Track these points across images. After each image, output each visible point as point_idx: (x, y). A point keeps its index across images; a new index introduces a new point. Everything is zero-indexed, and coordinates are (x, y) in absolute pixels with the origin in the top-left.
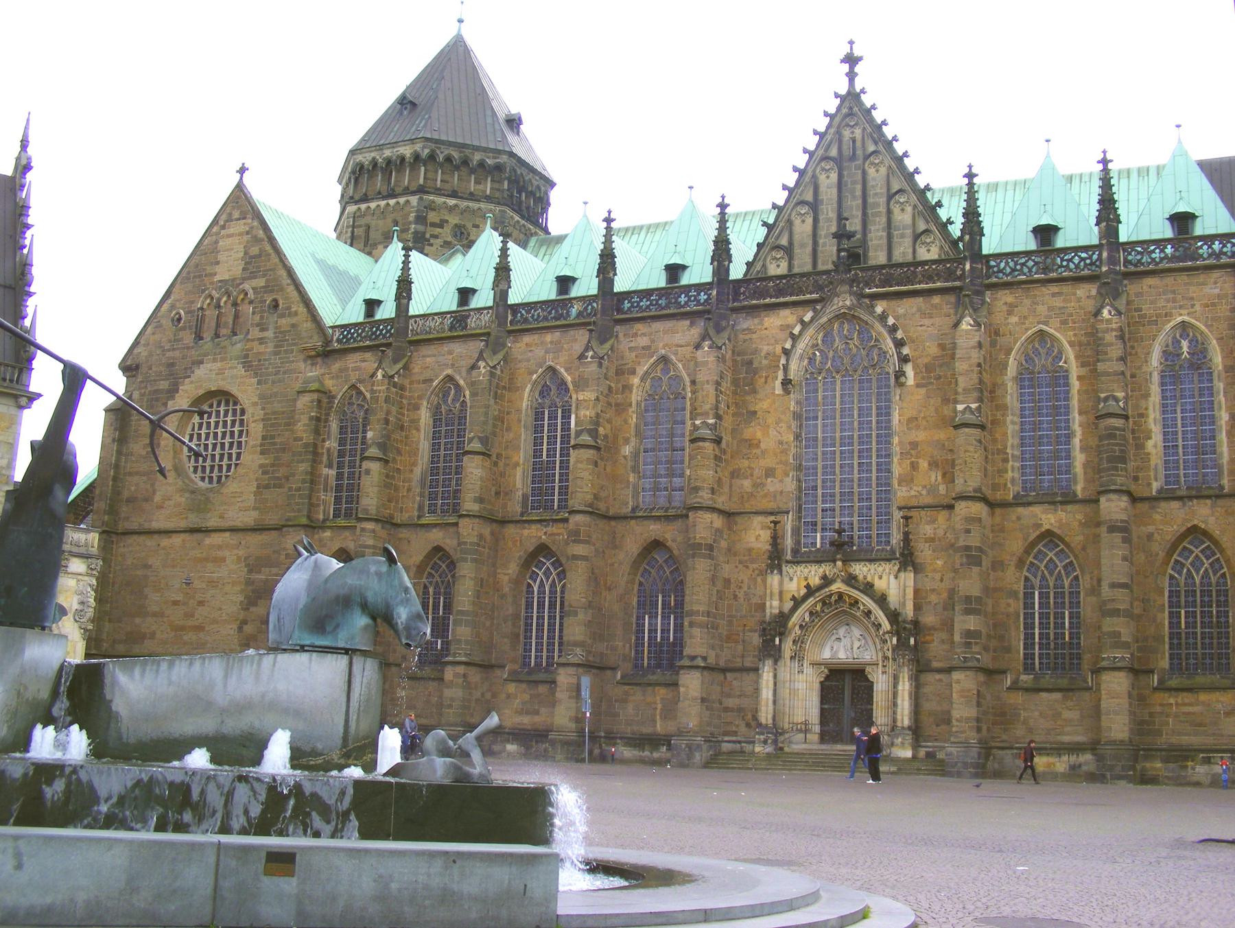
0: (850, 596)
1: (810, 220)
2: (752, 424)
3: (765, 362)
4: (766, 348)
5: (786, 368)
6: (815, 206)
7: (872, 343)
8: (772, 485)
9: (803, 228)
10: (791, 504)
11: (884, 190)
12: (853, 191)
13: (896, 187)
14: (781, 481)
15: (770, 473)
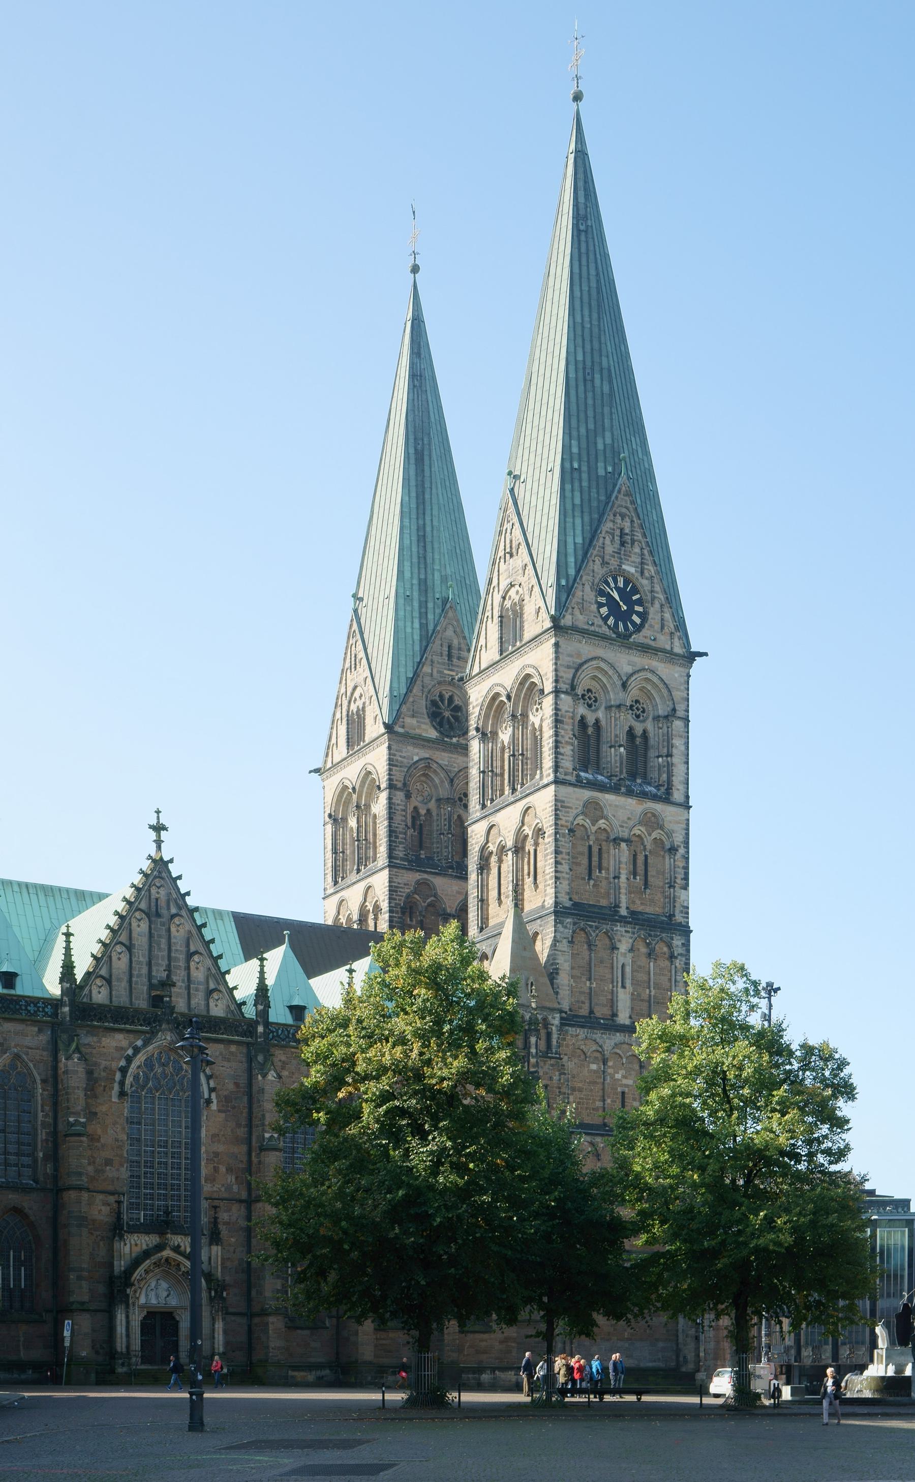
0: (175, 1260)
1: (125, 958)
2: (94, 1122)
3: (103, 1074)
4: (104, 1063)
5: (122, 1083)
6: (129, 948)
7: (183, 1073)
8: (110, 1172)
9: (120, 964)
10: (125, 1188)
11: (184, 949)
12: (159, 944)
13: (192, 949)
14: (118, 1170)
15: (109, 1162)
